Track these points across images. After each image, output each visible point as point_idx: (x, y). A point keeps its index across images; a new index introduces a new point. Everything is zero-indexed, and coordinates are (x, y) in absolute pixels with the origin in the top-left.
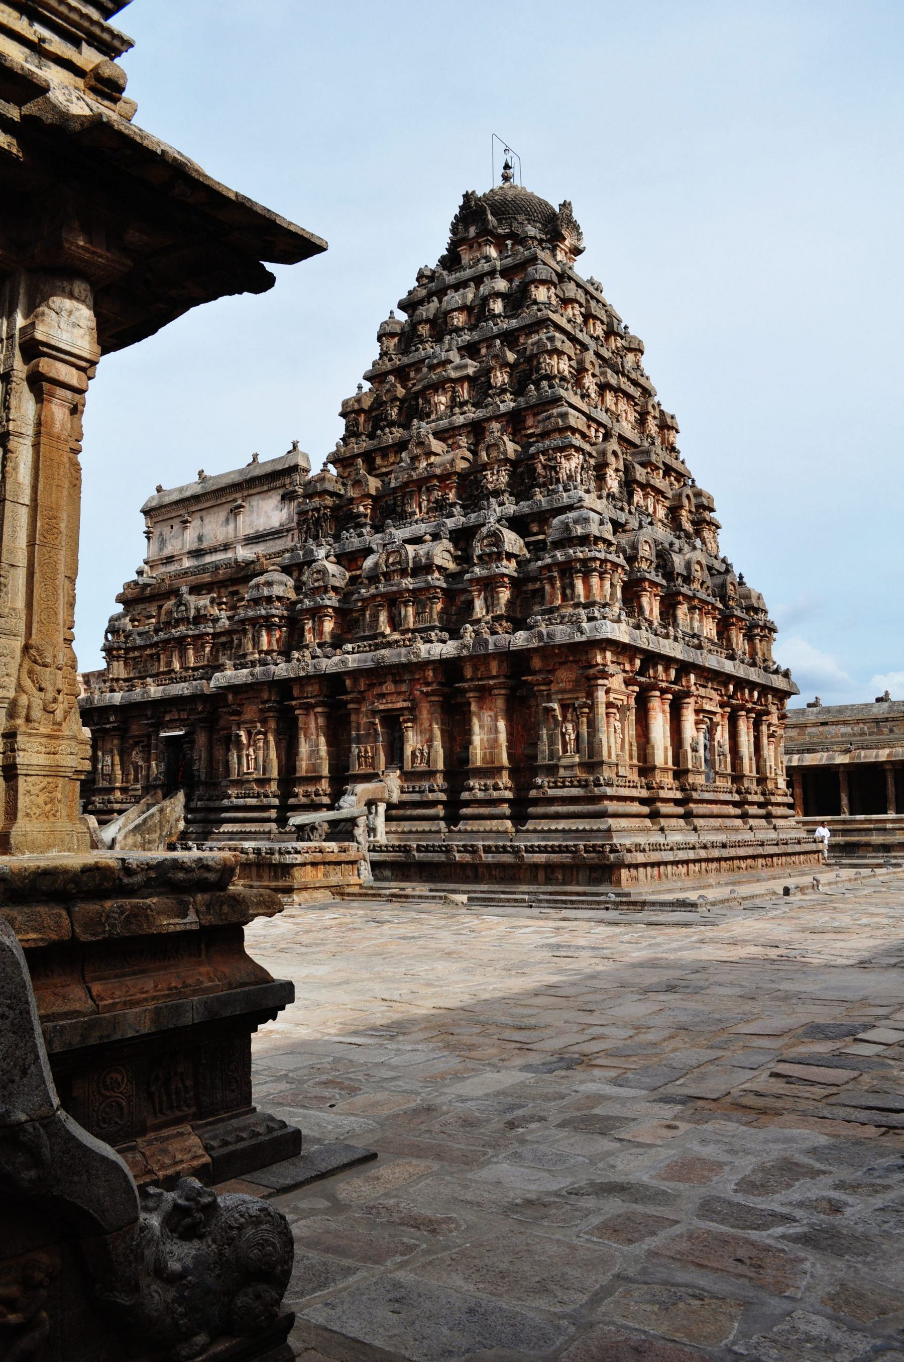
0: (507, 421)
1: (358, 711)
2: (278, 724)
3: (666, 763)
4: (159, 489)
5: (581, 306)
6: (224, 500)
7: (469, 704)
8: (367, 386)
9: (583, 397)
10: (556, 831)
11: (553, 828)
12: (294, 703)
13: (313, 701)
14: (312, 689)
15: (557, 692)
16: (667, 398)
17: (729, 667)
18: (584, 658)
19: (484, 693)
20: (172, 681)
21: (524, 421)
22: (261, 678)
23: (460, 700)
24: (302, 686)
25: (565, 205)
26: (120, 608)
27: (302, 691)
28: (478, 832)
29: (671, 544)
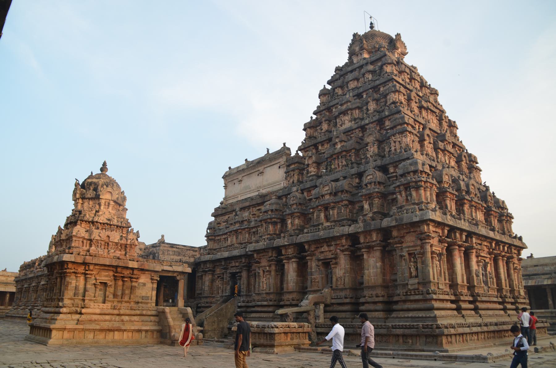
0: (377, 124)
2: (276, 267)
3: (463, 282)
4: (230, 168)
5: (408, 74)
6: (255, 170)
7: (363, 255)
9: (411, 111)
10: (408, 317)
11: (406, 316)
12: (282, 257)
13: (290, 256)
14: (290, 251)
15: (406, 247)
16: (451, 114)
17: (491, 234)
18: (418, 229)
19: (370, 248)
21: (384, 124)
23: (359, 253)
24: (286, 249)
25: (398, 35)
26: (213, 219)
27: (286, 252)
29: (459, 177)
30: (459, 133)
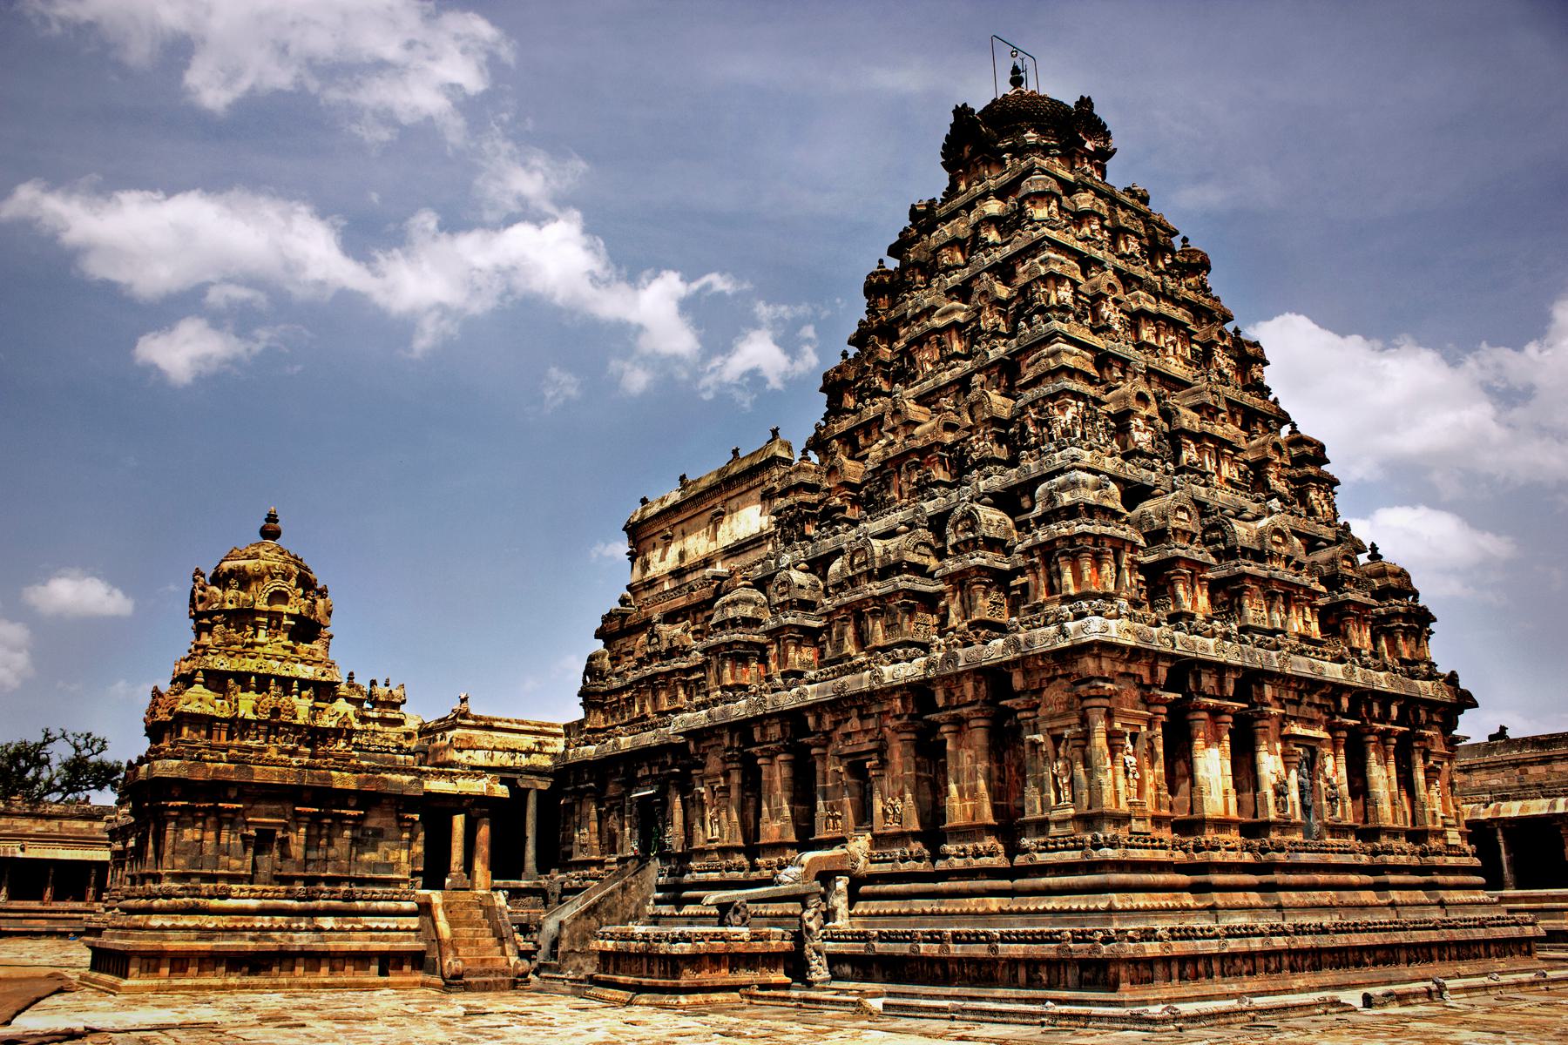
1: (824, 756)
3: (1227, 812)
8: (853, 351)
10: (1045, 911)
11: (1041, 907)
12: (753, 750)
20: (644, 729)
22: (719, 721)
26: (599, 645)
27: (763, 735)
28: (953, 914)
30: (1269, 376)
